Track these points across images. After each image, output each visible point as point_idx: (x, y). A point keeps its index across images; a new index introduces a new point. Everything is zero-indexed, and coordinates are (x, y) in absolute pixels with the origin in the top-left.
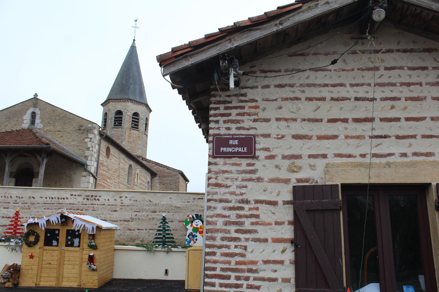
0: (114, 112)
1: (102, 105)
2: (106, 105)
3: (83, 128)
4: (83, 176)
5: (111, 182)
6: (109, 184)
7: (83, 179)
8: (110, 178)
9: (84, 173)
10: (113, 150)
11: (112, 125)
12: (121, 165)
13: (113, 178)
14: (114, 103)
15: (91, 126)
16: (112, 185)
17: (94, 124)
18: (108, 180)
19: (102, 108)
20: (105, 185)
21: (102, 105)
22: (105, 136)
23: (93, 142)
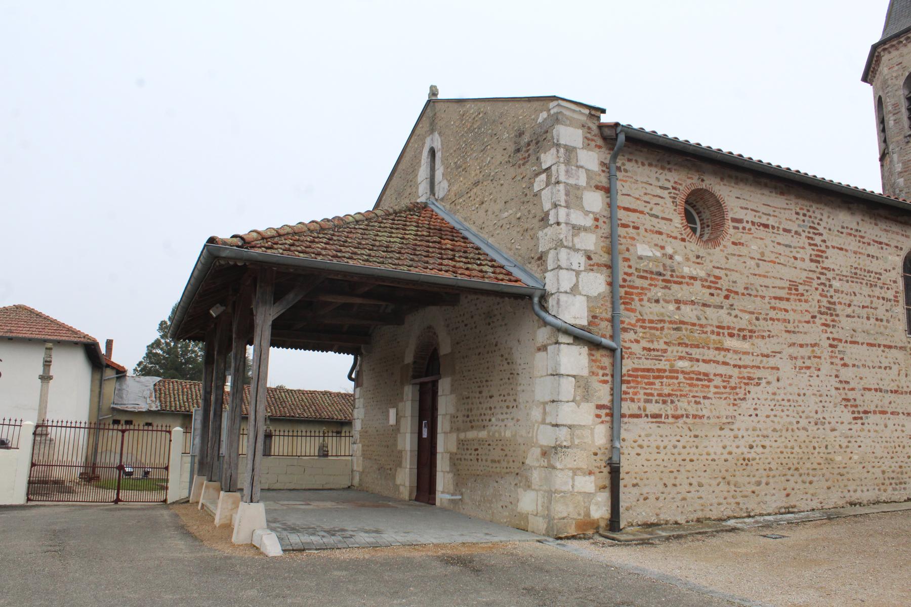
0: (901, 82)
1: (865, 79)
2: (875, 72)
3: (526, 138)
4: (539, 349)
5: (764, 346)
6: (747, 360)
7: (541, 362)
8: (745, 334)
9: (543, 335)
10: (735, 199)
11: (902, 129)
12: (834, 260)
13: (777, 328)
14: (895, 53)
15: (544, 115)
16: (772, 362)
17: (552, 104)
18: (729, 343)
19: (868, 89)
20: (703, 368)
21: (865, 79)
22: (622, 138)
23: (558, 183)
